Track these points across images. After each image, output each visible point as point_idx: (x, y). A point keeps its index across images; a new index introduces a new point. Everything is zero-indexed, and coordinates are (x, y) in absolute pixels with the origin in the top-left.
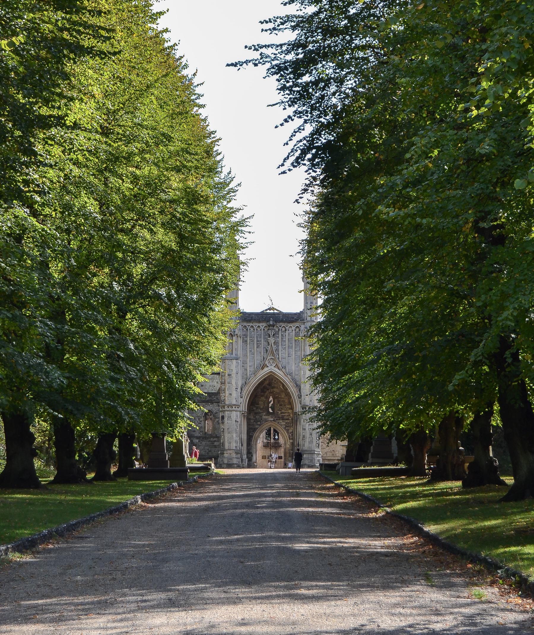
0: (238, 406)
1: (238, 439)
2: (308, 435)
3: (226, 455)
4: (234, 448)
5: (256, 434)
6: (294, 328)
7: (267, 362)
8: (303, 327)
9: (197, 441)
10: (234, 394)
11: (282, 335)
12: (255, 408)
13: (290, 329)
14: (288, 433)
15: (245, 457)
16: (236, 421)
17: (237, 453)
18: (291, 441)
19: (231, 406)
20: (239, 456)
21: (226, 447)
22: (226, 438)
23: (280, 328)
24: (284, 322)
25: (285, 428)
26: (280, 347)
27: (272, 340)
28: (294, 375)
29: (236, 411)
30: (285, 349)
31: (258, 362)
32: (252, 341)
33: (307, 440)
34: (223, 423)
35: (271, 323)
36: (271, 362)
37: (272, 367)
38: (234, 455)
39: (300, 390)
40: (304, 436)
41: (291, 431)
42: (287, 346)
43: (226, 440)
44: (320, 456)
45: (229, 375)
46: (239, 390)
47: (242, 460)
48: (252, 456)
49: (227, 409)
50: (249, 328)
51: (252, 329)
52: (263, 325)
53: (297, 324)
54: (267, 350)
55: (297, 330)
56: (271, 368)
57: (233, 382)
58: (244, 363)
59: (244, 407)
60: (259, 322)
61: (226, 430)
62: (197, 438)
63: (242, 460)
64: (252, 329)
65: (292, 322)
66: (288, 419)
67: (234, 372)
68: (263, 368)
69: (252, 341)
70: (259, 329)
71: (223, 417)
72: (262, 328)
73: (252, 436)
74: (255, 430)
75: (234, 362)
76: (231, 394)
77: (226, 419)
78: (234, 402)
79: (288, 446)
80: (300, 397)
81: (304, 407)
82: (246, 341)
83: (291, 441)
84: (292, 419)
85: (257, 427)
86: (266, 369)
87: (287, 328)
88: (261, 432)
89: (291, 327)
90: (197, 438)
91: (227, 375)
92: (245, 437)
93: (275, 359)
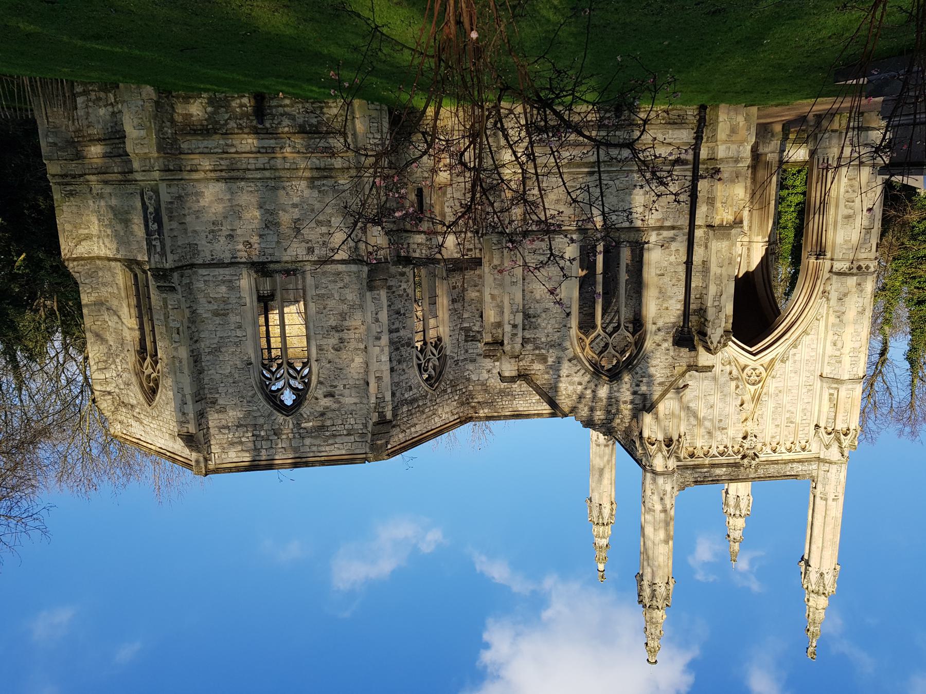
36: (754, 378)
37: (752, 364)
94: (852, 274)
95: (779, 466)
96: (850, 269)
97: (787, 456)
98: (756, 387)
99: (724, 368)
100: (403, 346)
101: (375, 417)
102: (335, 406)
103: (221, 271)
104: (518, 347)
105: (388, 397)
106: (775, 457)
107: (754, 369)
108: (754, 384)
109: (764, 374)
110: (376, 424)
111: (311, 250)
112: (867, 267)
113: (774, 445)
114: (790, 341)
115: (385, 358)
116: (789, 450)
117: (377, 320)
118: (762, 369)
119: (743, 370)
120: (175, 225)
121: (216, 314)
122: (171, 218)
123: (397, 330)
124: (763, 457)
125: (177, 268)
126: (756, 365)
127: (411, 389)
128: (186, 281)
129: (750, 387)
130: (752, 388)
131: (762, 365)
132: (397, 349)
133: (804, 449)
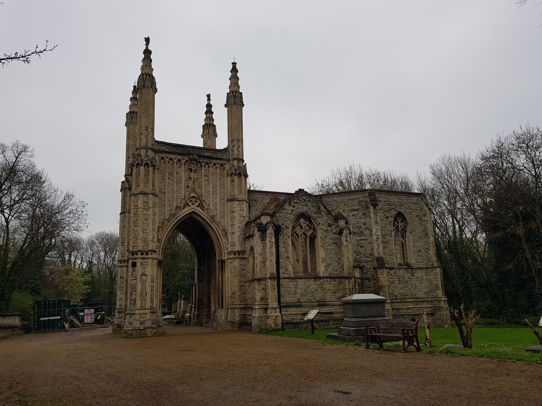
8: (227, 166)
94: (150, 251)
95: (176, 151)
96: (152, 254)
97: (173, 156)
98: (192, 195)
99: (208, 207)
100: (358, 233)
101: (378, 208)
102: (385, 213)
103: (420, 266)
104: (344, 232)
105: (372, 215)
106: (179, 157)
107: (193, 204)
108: (193, 197)
109: (188, 201)
110: (378, 205)
111: (395, 273)
112: (142, 254)
113: (179, 163)
114: (175, 217)
115: (374, 230)
116: (171, 159)
117: (378, 245)
118: (190, 204)
119: (199, 204)
120: (435, 283)
121: (420, 251)
122: (437, 285)
123: (362, 240)
124: (186, 158)
125: (435, 268)
127: (353, 215)
128: (431, 263)
130: (193, 195)
131: (189, 206)
132: (361, 232)
133: (163, 158)
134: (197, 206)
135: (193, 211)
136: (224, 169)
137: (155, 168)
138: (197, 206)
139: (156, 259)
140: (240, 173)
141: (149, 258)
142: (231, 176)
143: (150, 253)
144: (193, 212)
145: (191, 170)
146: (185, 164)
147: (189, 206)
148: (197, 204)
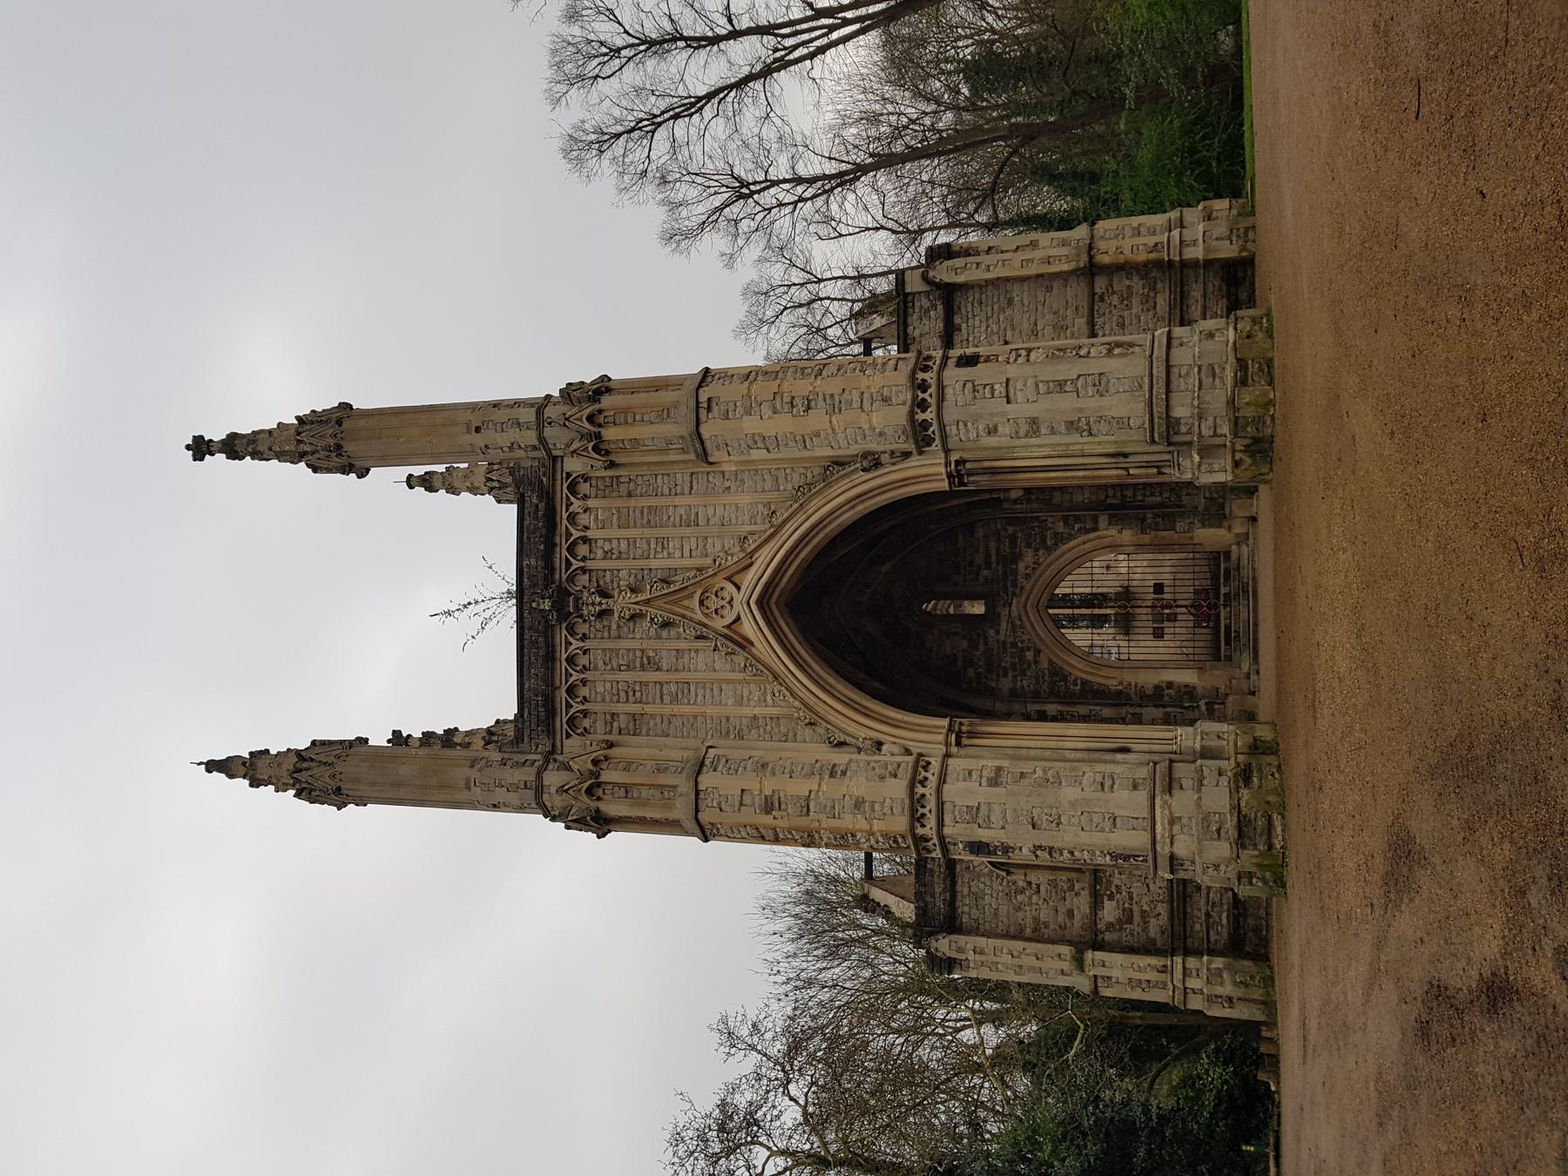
0: (921, 763)
1: (1091, 774)
2: (1065, 404)
3: (1182, 848)
4: (1142, 796)
5: (1078, 670)
6: (577, 505)
7: (719, 624)
8: (574, 465)
9: (1107, 903)
10: (857, 786)
11: (607, 555)
12: (971, 672)
13: (583, 519)
14: (1071, 537)
15: (1187, 738)
16: (994, 782)
17: (1171, 785)
18: (1103, 521)
19: (916, 802)
20: (1183, 771)
21: (1135, 840)
22: (1085, 838)
23: (576, 564)
24: (551, 546)
25: (1049, 550)
26: (654, 564)
27: (623, 602)
28: (772, 496)
29: (942, 779)
30: (663, 542)
31: (719, 661)
32: (631, 692)
33: (1091, 403)
34: (1006, 849)
35: (546, 605)
36: (713, 603)
37: (739, 598)
38: (1183, 802)
39: (839, 463)
40: (1072, 426)
41: (1060, 527)
42: (648, 532)
43: (1098, 839)
44: (1178, 331)
45: (769, 806)
46: (841, 758)
47: (1206, 753)
48: (1170, 685)
49: (931, 822)
50: (576, 707)
51: (584, 691)
52: (567, 642)
53: (562, 489)
54: (666, 625)
55: (584, 488)
56: (740, 605)
57: (800, 787)
58: (726, 729)
59: (928, 734)
60: (550, 657)
61: (1045, 839)
62: (1096, 904)
63: (1206, 753)
64: (584, 691)
65: (551, 513)
66: (1013, 538)
67: (751, 782)
68: (744, 644)
69: (631, 692)
70: (583, 660)
71: (978, 848)
72: (575, 644)
73: (1085, 683)
74: (1057, 673)
75: (706, 780)
76: (859, 804)
77: (983, 835)
78: (897, 789)
79: (1127, 535)
80: (873, 462)
81: (920, 436)
82: (634, 717)
83: (1103, 521)
84: (1011, 521)
85: (1044, 664)
86: (748, 628)
87: (576, 534)
88: (1067, 646)
89: (572, 518)
90: (1096, 904)
91: (768, 820)
92: (1077, 733)
93: (703, 584)
108: (701, 603)
119: (729, 579)
124: (561, 634)
126: (739, 608)
129: (697, 595)
131: (738, 619)
133: (571, 722)
134: (739, 588)
135: (759, 603)
136: (586, 479)
137: (606, 758)
138: (739, 588)
139: (947, 755)
140: (590, 419)
141: (939, 791)
142: (607, 453)
143: (920, 790)
144: (760, 603)
145: (604, 614)
146: (584, 637)
147: (738, 619)
148: (730, 587)
